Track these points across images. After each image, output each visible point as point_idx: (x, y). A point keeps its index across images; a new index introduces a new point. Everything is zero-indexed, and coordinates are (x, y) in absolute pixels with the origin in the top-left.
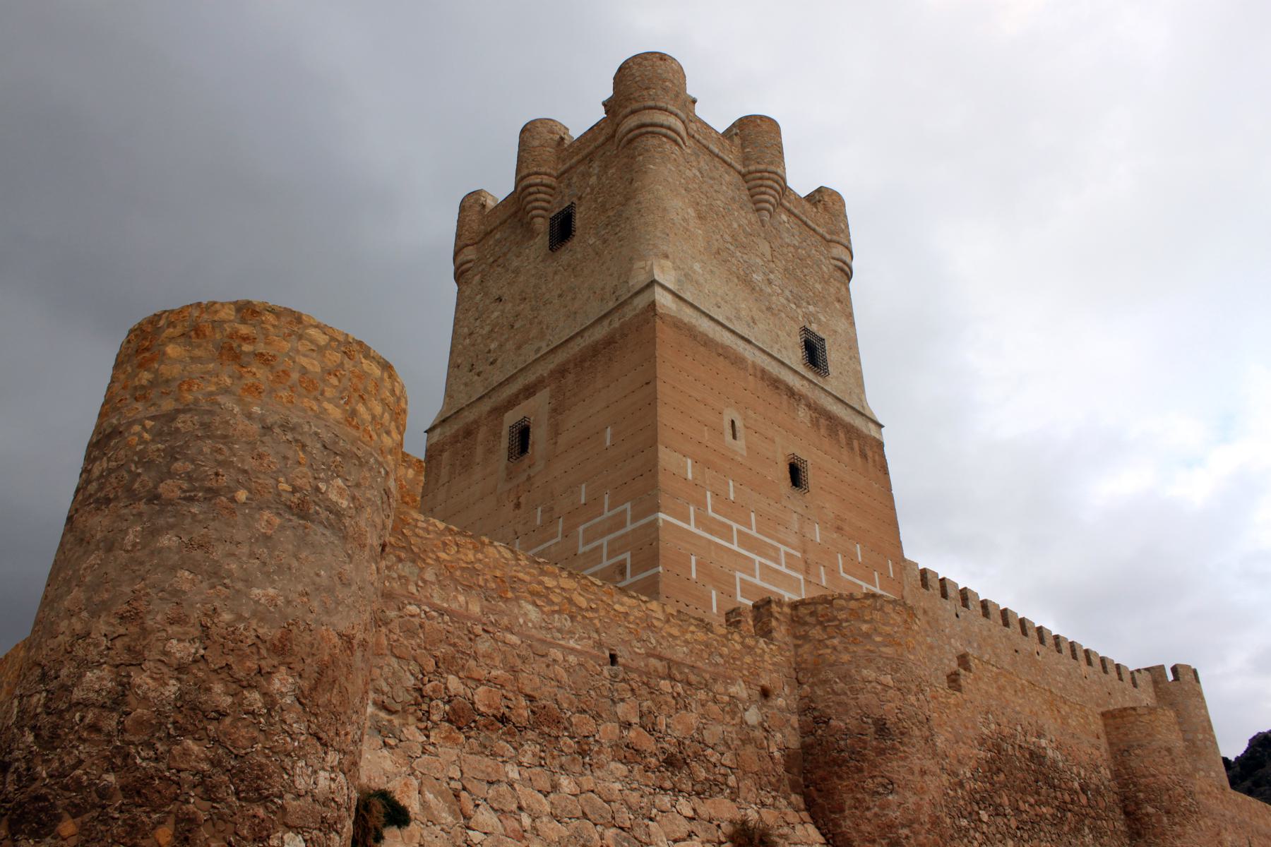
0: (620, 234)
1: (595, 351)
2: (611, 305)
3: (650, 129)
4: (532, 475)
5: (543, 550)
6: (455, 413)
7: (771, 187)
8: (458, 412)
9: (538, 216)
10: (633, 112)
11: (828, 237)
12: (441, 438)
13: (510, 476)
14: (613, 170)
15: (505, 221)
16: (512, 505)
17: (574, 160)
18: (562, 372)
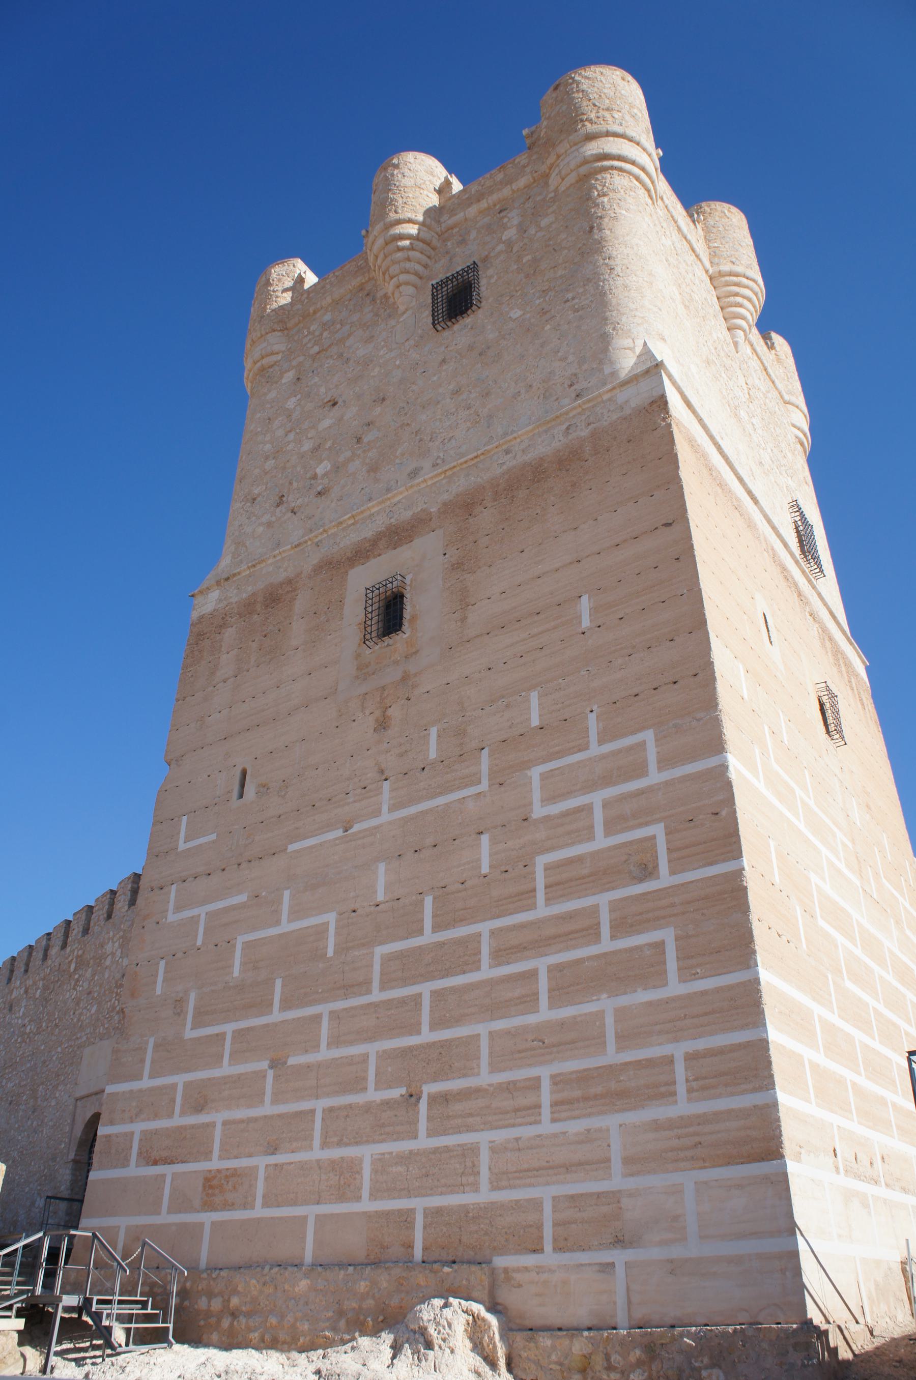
3: (616, 163)
7: (749, 300)
11: (787, 397)
12: (221, 605)
13: (363, 671)
16: (371, 721)
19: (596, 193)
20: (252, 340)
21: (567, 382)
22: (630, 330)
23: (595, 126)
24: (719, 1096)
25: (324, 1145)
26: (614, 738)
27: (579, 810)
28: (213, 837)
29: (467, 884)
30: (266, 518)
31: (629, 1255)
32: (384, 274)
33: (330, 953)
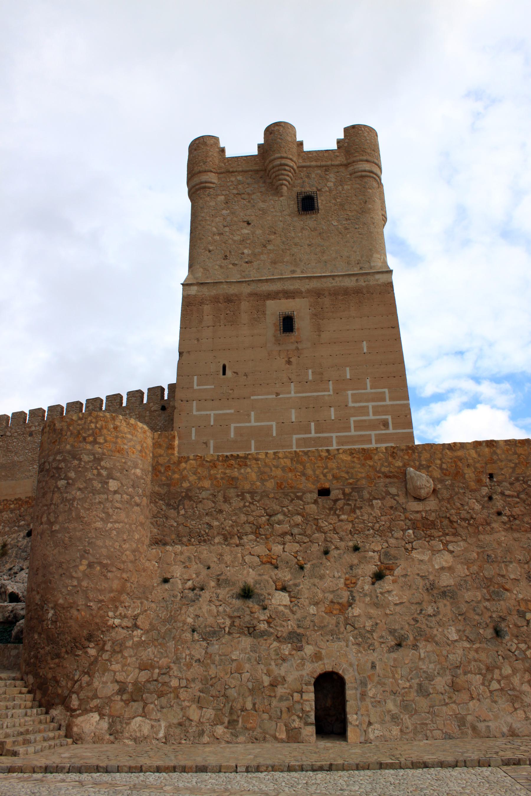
0: (359, 230)
1: (346, 292)
2: (356, 271)
3: (375, 176)
4: (300, 348)
5: (318, 396)
6: (214, 283)
8: (216, 283)
10: (367, 161)
14: (349, 187)
15: (246, 172)
16: (284, 361)
17: (313, 163)
18: (318, 294)
21: (356, 262)
26: (375, 388)
28: (213, 387)
29: (327, 421)
30: (218, 262)
33: (274, 435)
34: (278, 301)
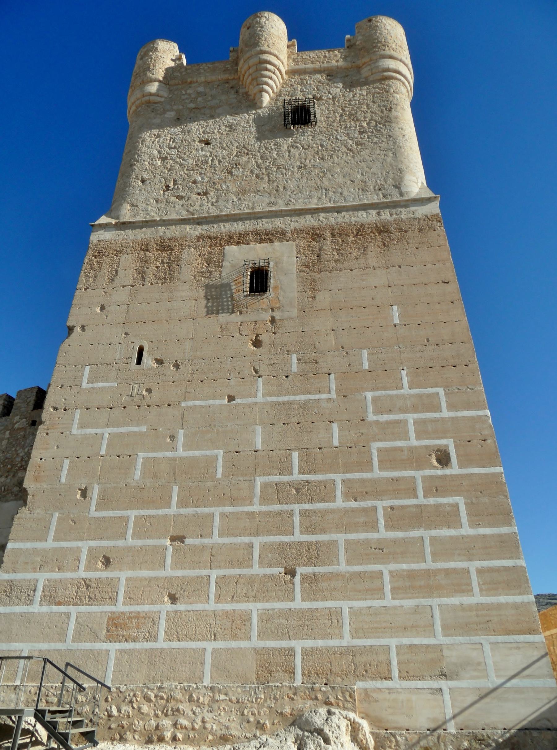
4: (277, 317)
5: (308, 401)
9: (267, 92)
19: (392, 91)
20: (143, 81)
22: (415, 173)
23: (395, 53)
24: (500, 595)
25: (218, 600)
27: (398, 422)
31: (451, 683)
32: (253, 80)
33: (219, 475)
34: (244, 246)
